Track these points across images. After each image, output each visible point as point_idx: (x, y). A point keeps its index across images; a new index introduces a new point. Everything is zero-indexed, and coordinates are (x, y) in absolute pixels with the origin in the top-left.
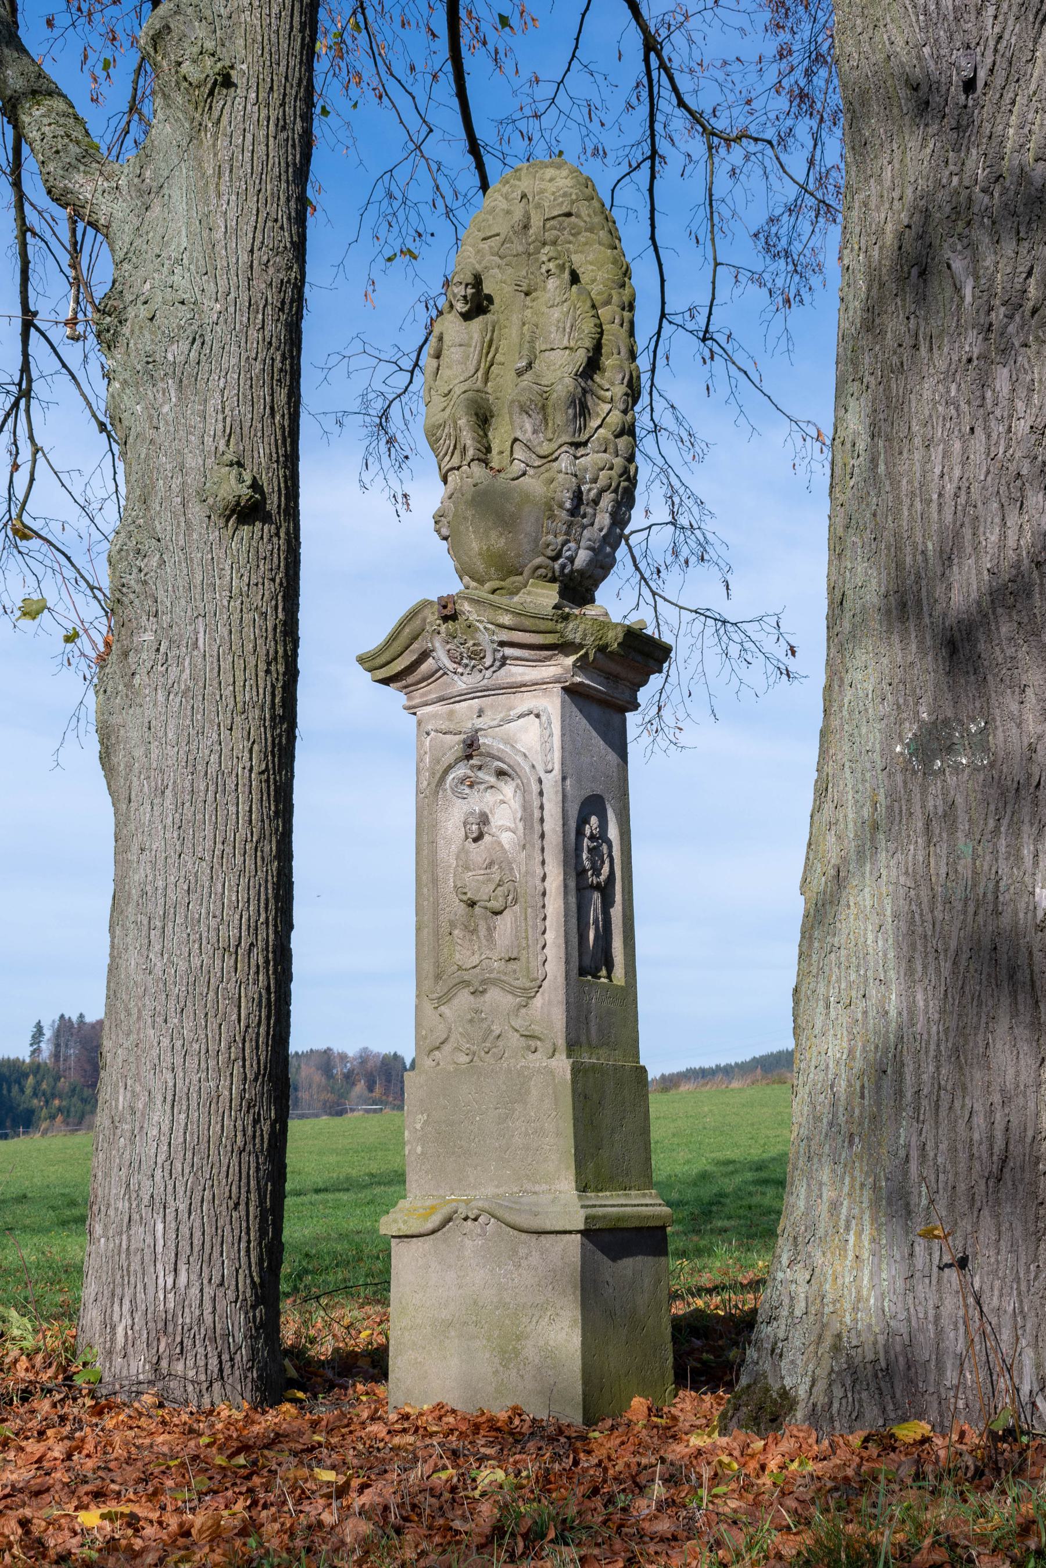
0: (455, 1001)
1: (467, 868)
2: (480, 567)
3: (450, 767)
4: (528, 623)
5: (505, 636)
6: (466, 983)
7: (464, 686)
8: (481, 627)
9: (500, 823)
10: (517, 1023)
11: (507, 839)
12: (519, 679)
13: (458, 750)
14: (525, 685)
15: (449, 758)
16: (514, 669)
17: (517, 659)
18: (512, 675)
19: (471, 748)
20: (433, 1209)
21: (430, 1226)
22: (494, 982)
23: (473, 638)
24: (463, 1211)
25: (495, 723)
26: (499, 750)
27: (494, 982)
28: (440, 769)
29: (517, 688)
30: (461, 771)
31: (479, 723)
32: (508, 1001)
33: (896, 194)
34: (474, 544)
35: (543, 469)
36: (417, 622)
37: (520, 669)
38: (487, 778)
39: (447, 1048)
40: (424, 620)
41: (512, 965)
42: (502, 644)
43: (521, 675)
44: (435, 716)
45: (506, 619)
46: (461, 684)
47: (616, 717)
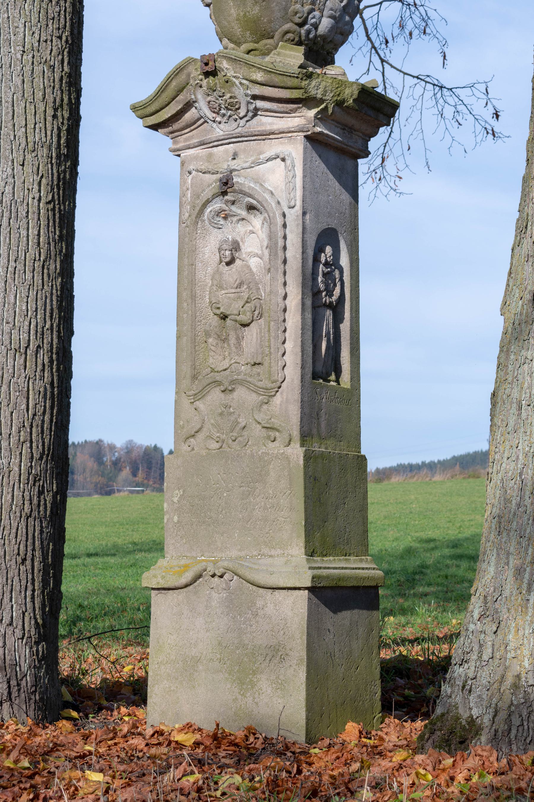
0: (209, 398)
1: (221, 287)
2: (238, 30)
3: (208, 202)
4: (277, 80)
5: (257, 90)
6: (217, 383)
7: (222, 133)
8: (237, 82)
9: (249, 250)
10: (259, 417)
11: (254, 263)
12: (268, 128)
13: (215, 187)
14: (273, 133)
15: (207, 194)
16: (264, 119)
17: (267, 110)
18: (262, 124)
19: (226, 185)
20: (186, 567)
21: (183, 581)
22: (242, 383)
23: (230, 92)
24: (211, 569)
25: (247, 165)
26: (249, 187)
27: (242, 383)
28: (199, 203)
29: (266, 135)
30: (217, 205)
31: (234, 165)
32: (252, 398)
34: (233, 11)
36: (182, 77)
37: (270, 120)
38: (239, 211)
39: (201, 436)
40: (189, 75)
41: (256, 369)
42: (255, 97)
43: (270, 124)
44: (196, 158)
45: (259, 76)
46: (219, 131)
47: (350, 163)
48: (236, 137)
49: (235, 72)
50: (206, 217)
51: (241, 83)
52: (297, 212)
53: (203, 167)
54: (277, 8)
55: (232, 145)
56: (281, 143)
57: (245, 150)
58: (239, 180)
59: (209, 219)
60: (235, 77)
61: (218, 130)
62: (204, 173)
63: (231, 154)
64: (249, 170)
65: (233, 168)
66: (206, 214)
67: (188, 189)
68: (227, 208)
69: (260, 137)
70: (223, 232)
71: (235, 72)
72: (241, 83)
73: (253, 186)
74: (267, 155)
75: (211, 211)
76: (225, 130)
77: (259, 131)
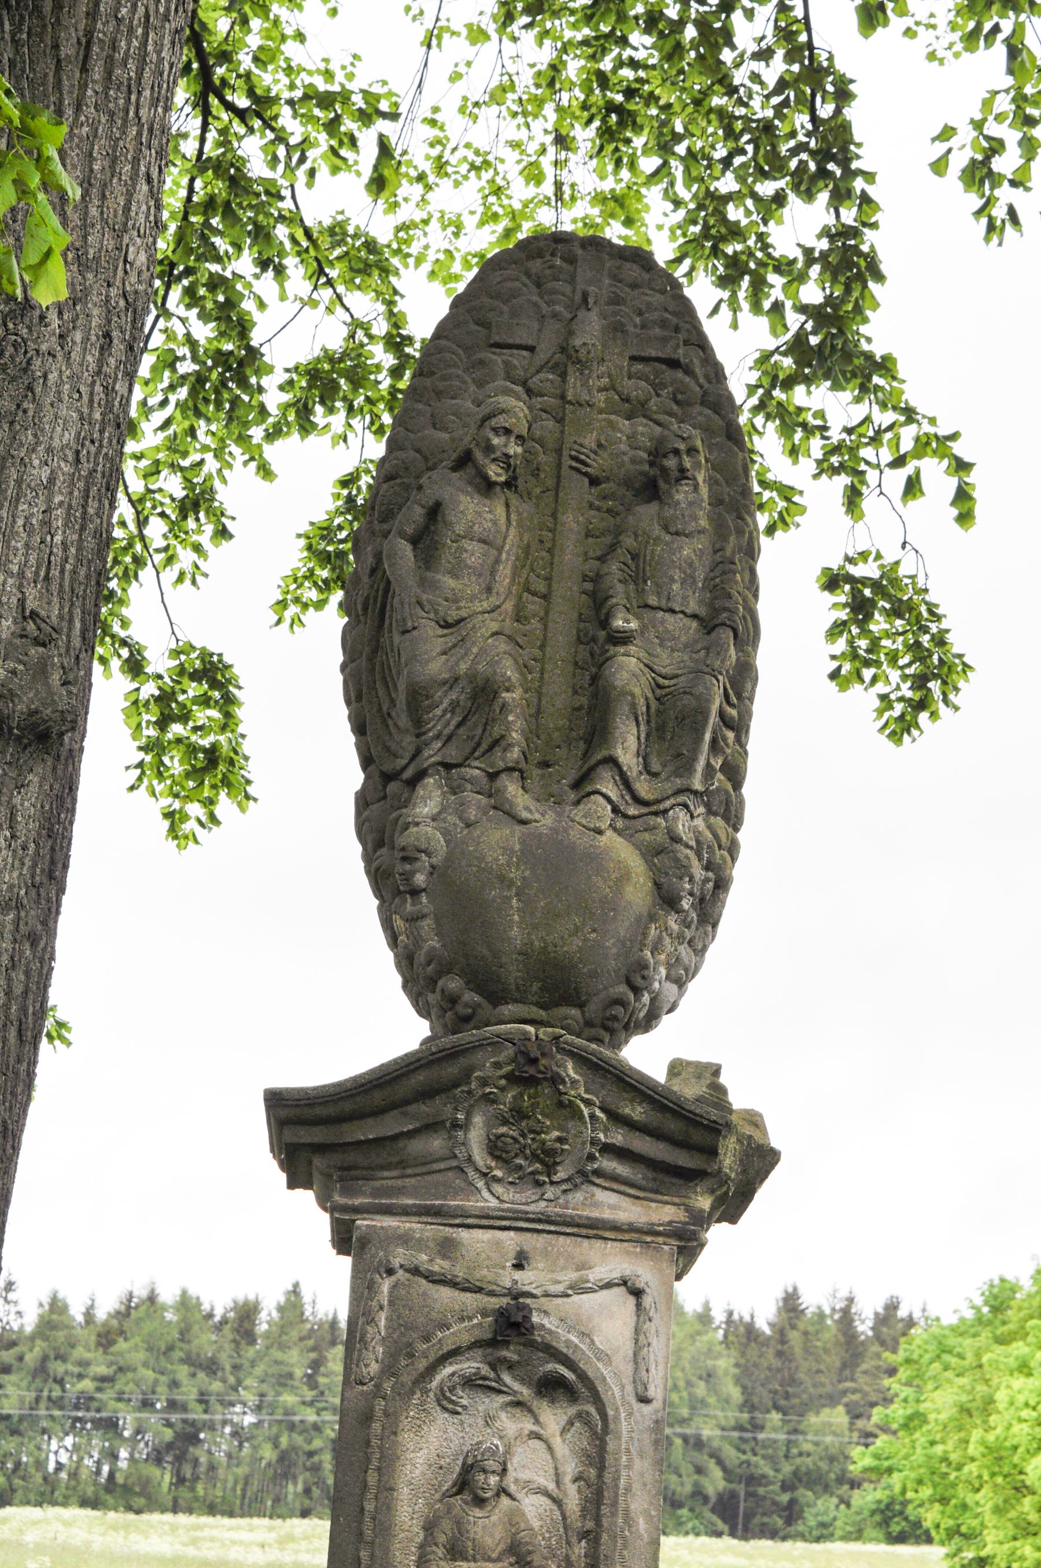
3: (454, 1353)
4: (673, 1126)
5: (618, 1137)
7: (493, 1203)
8: (586, 1112)
9: (524, 1475)
11: (534, 1509)
12: (607, 1215)
13: (480, 1326)
15: (459, 1333)
16: (601, 1195)
17: (615, 1178)
18: (596, 1205)
19: (512, 1327)
23: (560, 1128)
25: (559, 1288)
26: (568, 1342)
28: (426, 1351)
29: (595, 1229)
31: (527, 1279)
34: (515, 931)
35: (639, 824)
36: (451, 1070)
37: (612, 1198)
38: (516, 1386)
42: (607, 1149)
43: (612, 1207)
45: (636, 1112)
48: (528, 1220)
49: (587, 1091)
50: (434, 1384)
51: (592, 1116)
52: (657, 1411)
53: (436, 1268)
54: (614, 951)
55: (512, 1233)
56: (628, 1253)
57: (545, 1253)
58: (546, 1322)
59: (442, 1390)
60: (583, 1100)
61: (486, 1194)
62: (434, 1282)
63: (512, 1255)
64: (560, 1300)
65: (526, 1288)
66: (438, 1378)
67: (381, 1308)
68: (492, 1375)
69: (584, 1232)
70: (462, 1423)
71: (587, 1091)
72: (592, 1116)
73: (576, 1340)
74: (600, 1272)
75: (453, 1374)
76: (505, 1198)
77: (588, 1218)
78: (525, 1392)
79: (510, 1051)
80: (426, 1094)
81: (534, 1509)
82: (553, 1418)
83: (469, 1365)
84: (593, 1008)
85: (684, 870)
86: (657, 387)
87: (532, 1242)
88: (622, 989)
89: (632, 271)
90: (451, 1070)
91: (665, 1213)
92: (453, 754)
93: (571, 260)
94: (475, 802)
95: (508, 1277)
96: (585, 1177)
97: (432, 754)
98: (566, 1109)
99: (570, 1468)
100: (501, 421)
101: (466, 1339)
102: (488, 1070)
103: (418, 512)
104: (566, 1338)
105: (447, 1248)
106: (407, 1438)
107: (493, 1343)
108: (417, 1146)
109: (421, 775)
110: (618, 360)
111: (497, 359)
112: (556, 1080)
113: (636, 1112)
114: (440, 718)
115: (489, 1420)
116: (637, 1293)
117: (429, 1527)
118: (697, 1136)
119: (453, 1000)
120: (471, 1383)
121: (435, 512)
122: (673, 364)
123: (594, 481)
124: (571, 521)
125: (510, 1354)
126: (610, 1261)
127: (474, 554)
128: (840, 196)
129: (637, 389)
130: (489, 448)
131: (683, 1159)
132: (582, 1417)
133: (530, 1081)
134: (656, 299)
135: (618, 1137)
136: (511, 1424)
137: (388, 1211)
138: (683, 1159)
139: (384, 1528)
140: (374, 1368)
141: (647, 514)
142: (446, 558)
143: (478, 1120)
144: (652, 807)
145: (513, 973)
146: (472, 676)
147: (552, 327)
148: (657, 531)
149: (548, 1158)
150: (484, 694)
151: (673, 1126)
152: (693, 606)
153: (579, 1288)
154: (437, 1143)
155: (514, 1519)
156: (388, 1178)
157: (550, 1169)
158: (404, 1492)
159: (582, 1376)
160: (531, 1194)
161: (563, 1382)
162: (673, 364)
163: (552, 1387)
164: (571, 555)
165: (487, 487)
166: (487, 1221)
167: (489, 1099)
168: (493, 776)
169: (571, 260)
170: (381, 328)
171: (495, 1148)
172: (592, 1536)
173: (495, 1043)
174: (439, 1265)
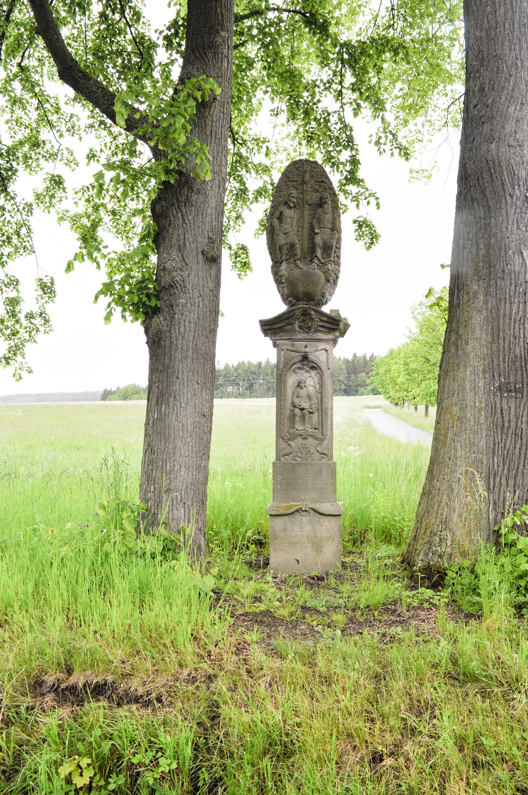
0: (296, 441)
3: (296, 363)
4: (331, 321)
5: (322, 324)
10: (318, 449)
11: (311, 389)
13: (300, 358)
15: (296, 360)
19: (305, 358)
20: (289, 507)
21: (289, 512)
28: (290, 363)
31: (307, 350)
33: (504, 226)
36: (292, 314)
39: (291, 456)
41: (316, 431)
42: (320, 326)
44: (285, 344)
45: (325, 319)
46: (299, 337)
78: (308, 369)
79: (301, 310)
80: (288, 318)
81: (311, 389)
82: (313, 373)
83: (298, 365)
84: (316, 301)
85: (330, 275)
86: (320, 186)
87: (308, 343)
88: (321, 298)
89: (314, 165)
90: (292, 314)
91: (331, 336)
92: (288, 257)
93: (303, 164)
94: (292, 266)
95: (304, 350)
96: (316, 331)
97: (284, 257)
98: (312, 319)
99: (317, 382)
100: (292, 195)
101: (297, 361)
102: (298, 313)
103: (278, 214)
104: (315, 360)
105: (293, 345)
106: (288, 378)
107: (302, 361)
108: (286, 328)
109: (282, 262)
110: (313, 182)
111: (290, 184)
112: (310, 314)
113: (325, 319)
114: (285, 251)
115: (302, 374)
116: (327, 351)
117: (293, 393)
118: (336, 323)
119: (291, 302)
120: (299, 368)
121: (281, 213)
122: (323, 182)
123: (310, 205)
124: (306, 213)
125: (305, 363)
126: (322, 346)
127: (289, 220)
128: (352, 149)
129: (317, 187)
130: (290, 200)
131: (334, 327)
132: (318, 373)
133: (306, 315)
134: (319, 170)
135: (322, 324)
136: (306, 375)
137: (282, 340)
138: (334, 327)
139: (285, 394)
140: (282, 367)
141: (320, 210)
142: (284, 221)
143: (297, 322)
144: (324, 264)
145: (301, 296)
146: (290, 243)
147: (300, 177)
148: (322, 213)
149: (309, 328)
150: (292, 246)
151: (331, 321)
152: (329, 227)
153: (316, 351)
154: (290, 327)
155: (308, 391)
156: (282, 334)
157: (310, 330)
158: (288, 387)
159: (318, 366)
160: (307, 335)
161: (315, 367)
162: (323, 182)
163: (313, 368)
164: (307, 219)
165: (290, 208)
166: (299, 340)
167: (298, 319)
168: (295, 261)
169: (303, 164)
170: (269, 182)
171: (300, 327)
172: (321, 393)
173: (299, 309)
174: (292, 348)
